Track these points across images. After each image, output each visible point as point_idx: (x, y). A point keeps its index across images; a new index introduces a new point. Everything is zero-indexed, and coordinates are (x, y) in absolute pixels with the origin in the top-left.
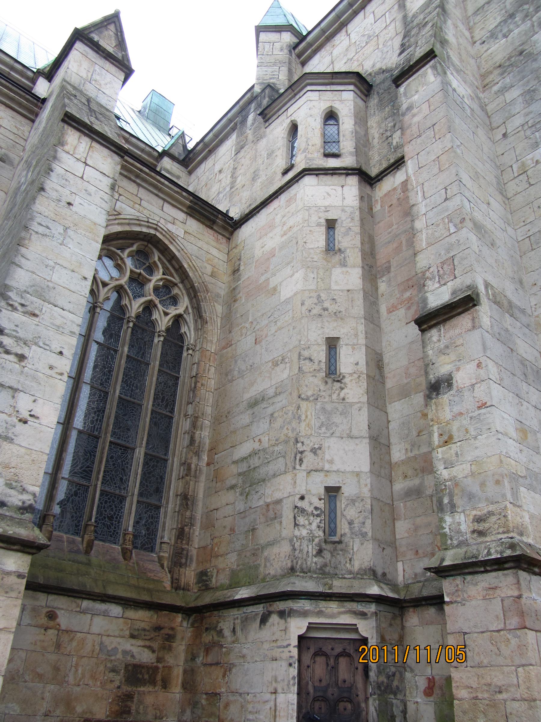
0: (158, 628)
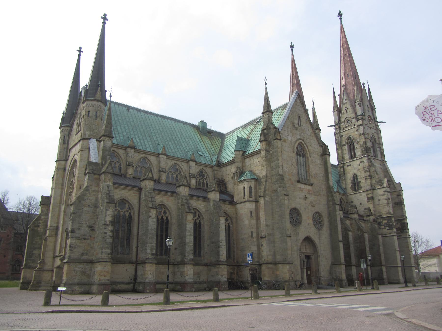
0: (233, 268)
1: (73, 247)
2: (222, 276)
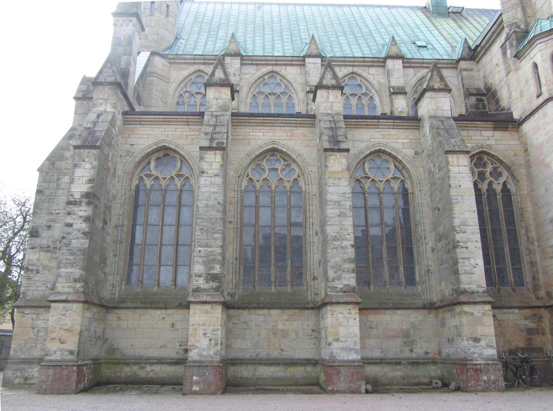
1: (32, 270)
2: (476, 340)
